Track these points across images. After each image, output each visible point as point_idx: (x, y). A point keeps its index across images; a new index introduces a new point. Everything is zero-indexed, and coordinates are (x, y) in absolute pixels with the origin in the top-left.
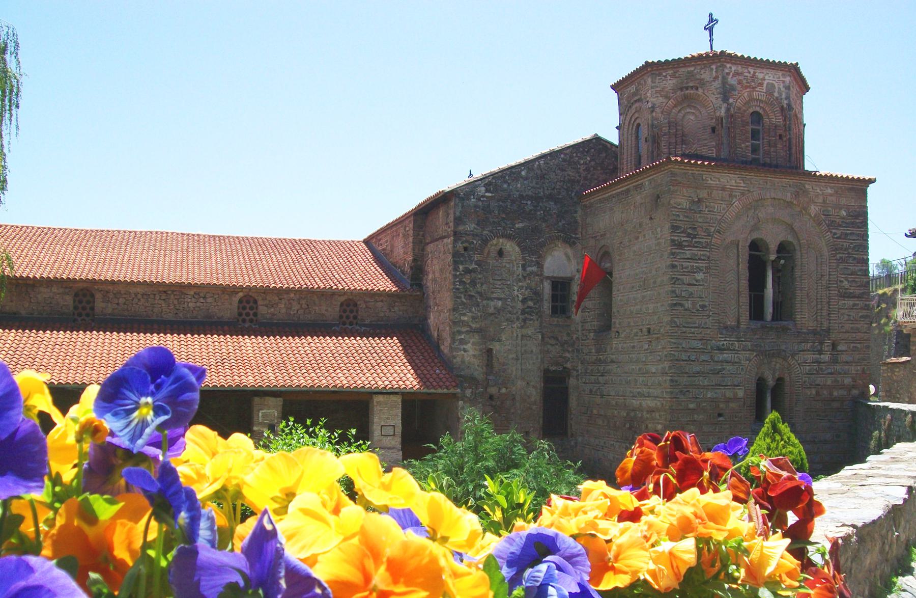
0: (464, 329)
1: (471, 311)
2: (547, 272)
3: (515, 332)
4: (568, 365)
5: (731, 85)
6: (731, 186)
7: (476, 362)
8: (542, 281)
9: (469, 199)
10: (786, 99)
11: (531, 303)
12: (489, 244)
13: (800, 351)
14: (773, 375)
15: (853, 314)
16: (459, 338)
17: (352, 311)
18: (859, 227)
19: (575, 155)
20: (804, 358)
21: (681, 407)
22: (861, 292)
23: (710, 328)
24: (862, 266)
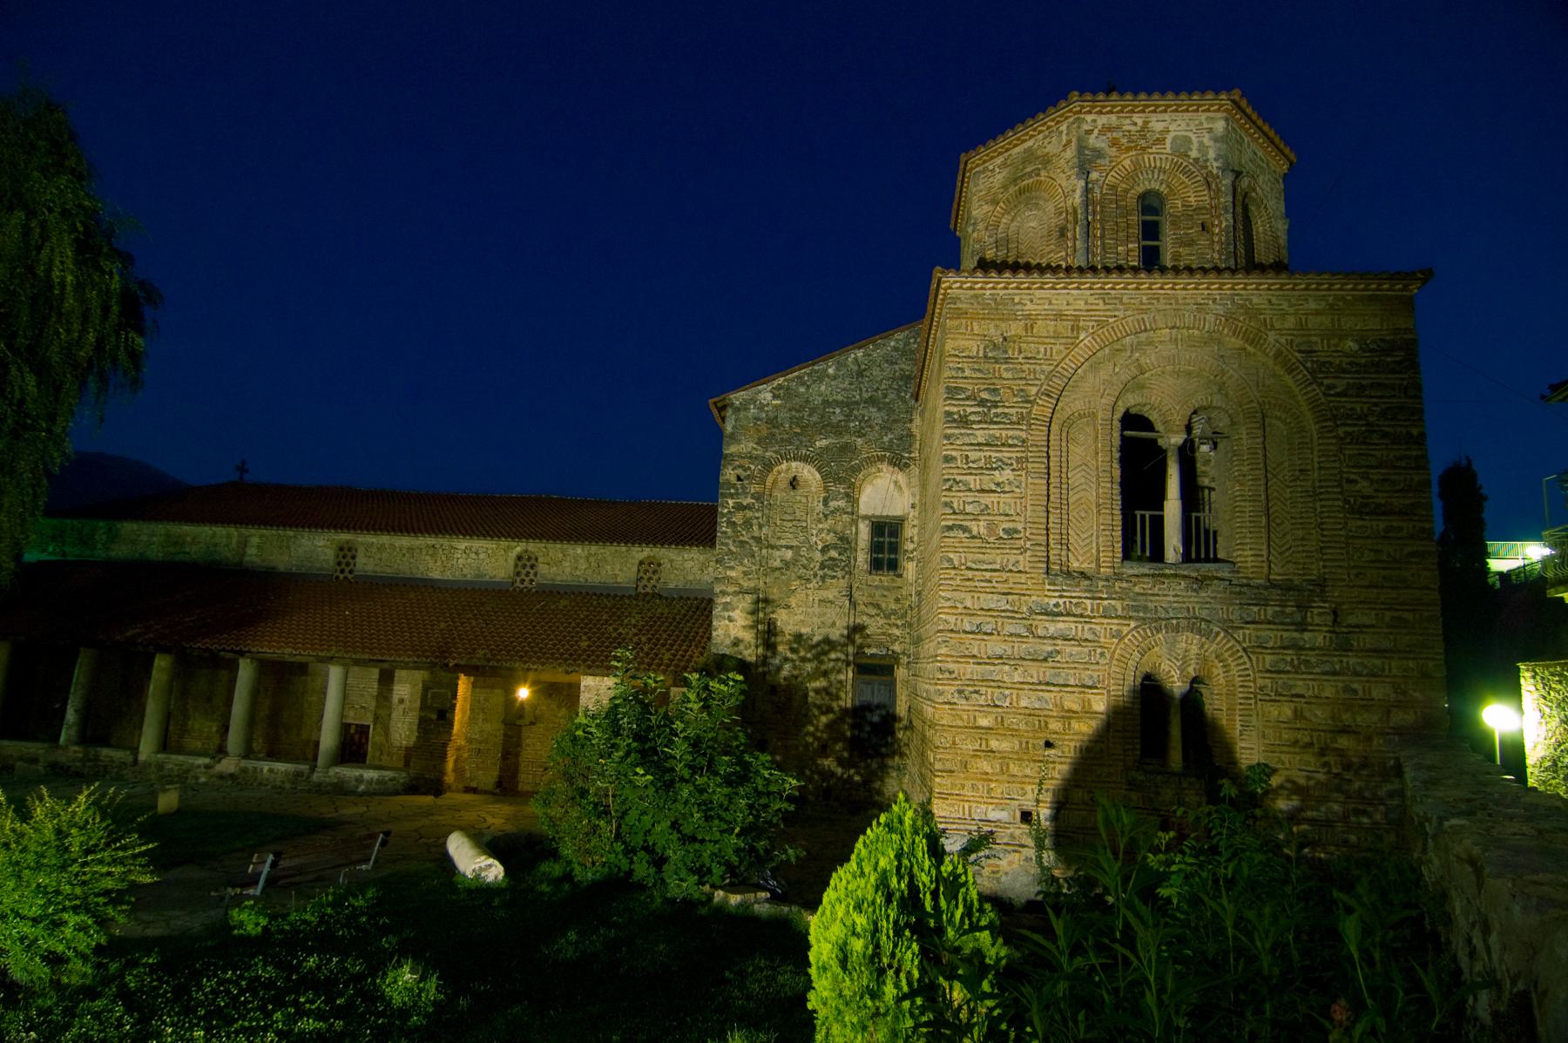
0: (731, 589)
1: (742, 564)
2: (863, 510)
4: (897, 647)
5: (1094, 150)
6: (1075, 310)
8: (855, 522)
9: (747, 409)
10: (1216, 160)
11: (833, 554)
12: (775, 469)
16: (724, 600)
18: (1392, 371)
19: (912, 341)
22: (1408, 502)
23: (1026, 572)
24: (1407, 449)
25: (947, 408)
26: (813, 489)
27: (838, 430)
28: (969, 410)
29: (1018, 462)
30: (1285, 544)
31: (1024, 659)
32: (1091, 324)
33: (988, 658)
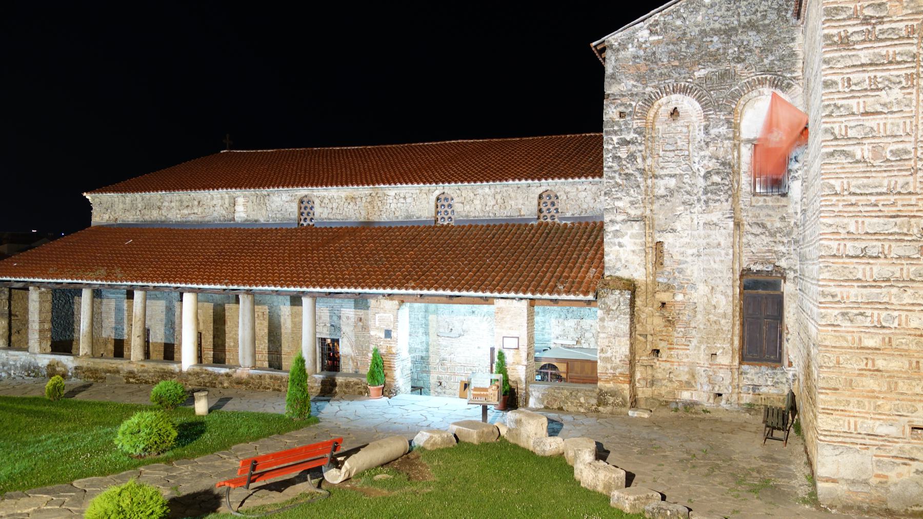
0: (620, 218)
1: (628, 194)
3: (696, 218)
4: (783, 263)
7: (637, 260)
8: (736, 147)
11: (716, 179)
21: (845, 344)
23: (917, 194)
25: (826, 31)
26: (694, 119)
27: (715, 58)
28: (850, 30)
31: (912, 280)
33: (875, 281)
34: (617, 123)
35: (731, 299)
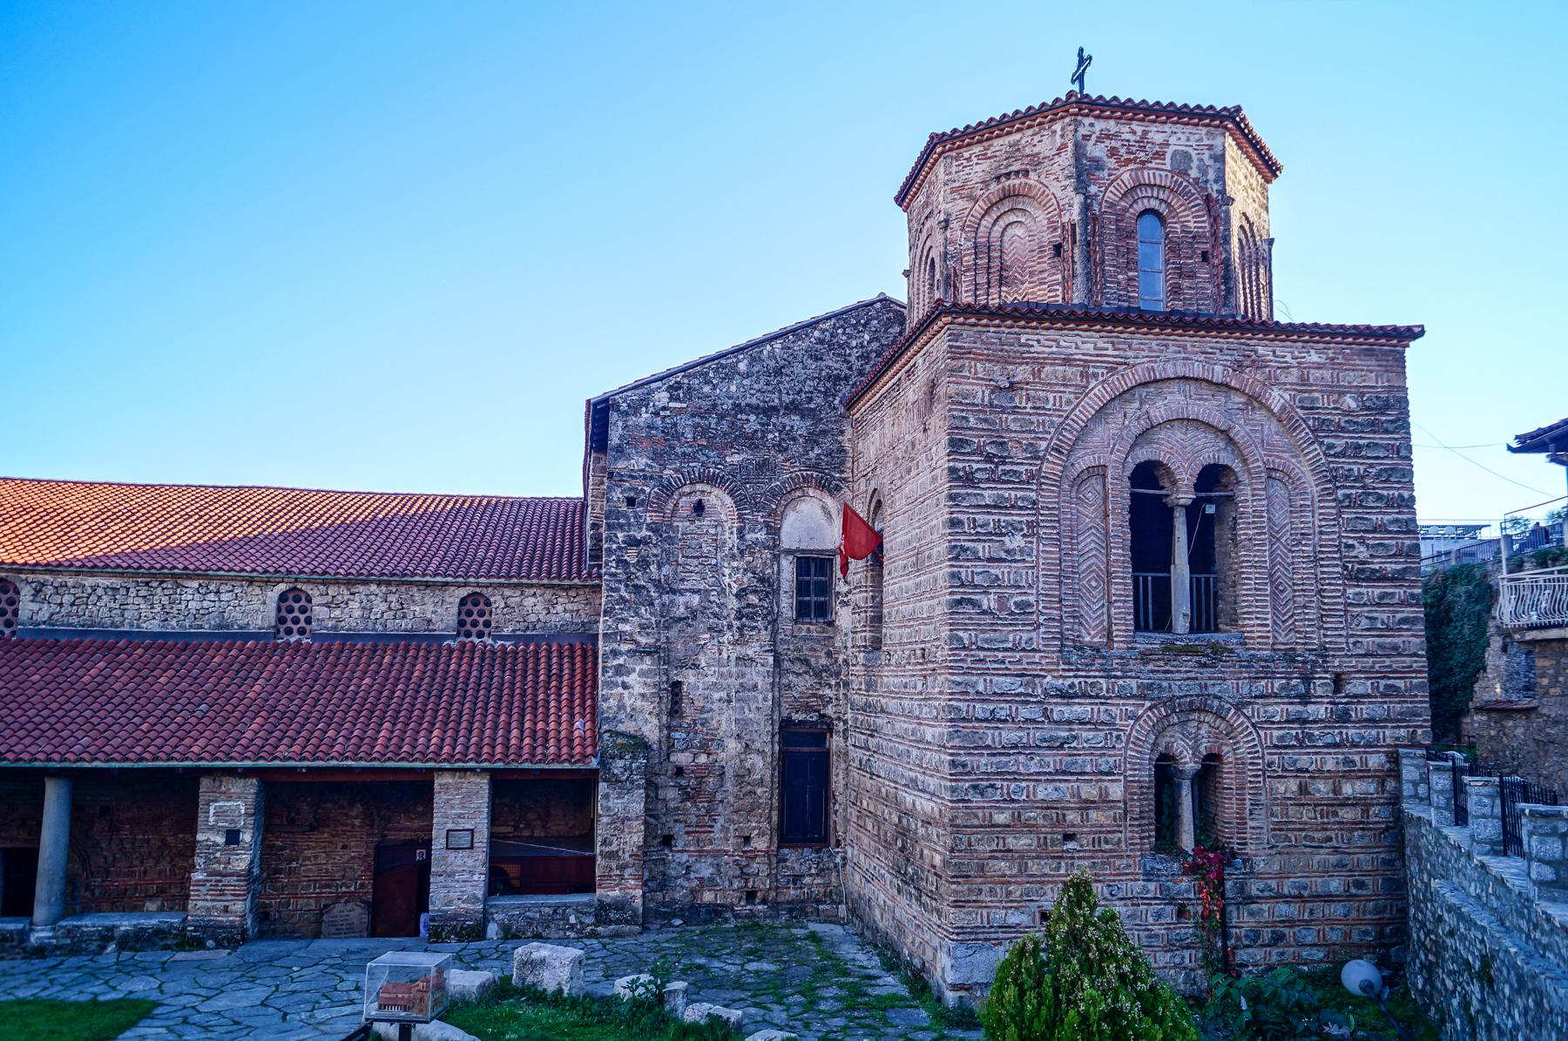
0: (624, 647)
1: (637, 614)
2: (786, 543)
4: (830, 711)
8: (776, 558)
10: (1216, 181)
11: (753, 599)
13: (1256, 697)
14: (1195, 749)
15: (1382, 615)
17: (482, 614)
18: (1386, 431)
19: (840, 331)
20: (1266, 712)
21: (976, 822)
22: (1399, 567)
23: (1040, 651)
25: (951, 464)
27: (752, 442)
28: (975, 466)
29: (1028, 528)
30: (1288, 611)
31: (1038, 746)
32: (1100, 371)
33: (1004, 747)
34: (625, 515)
35: (769, 760)
